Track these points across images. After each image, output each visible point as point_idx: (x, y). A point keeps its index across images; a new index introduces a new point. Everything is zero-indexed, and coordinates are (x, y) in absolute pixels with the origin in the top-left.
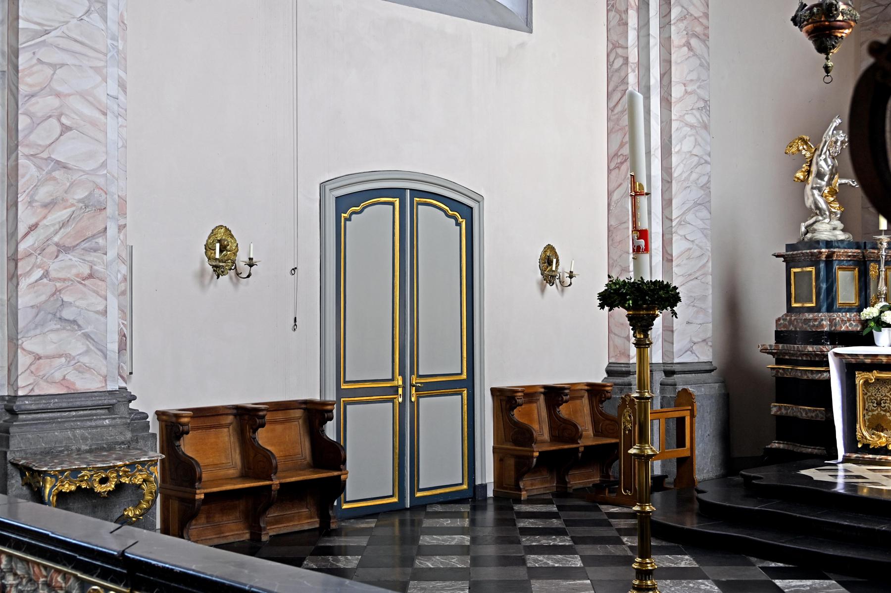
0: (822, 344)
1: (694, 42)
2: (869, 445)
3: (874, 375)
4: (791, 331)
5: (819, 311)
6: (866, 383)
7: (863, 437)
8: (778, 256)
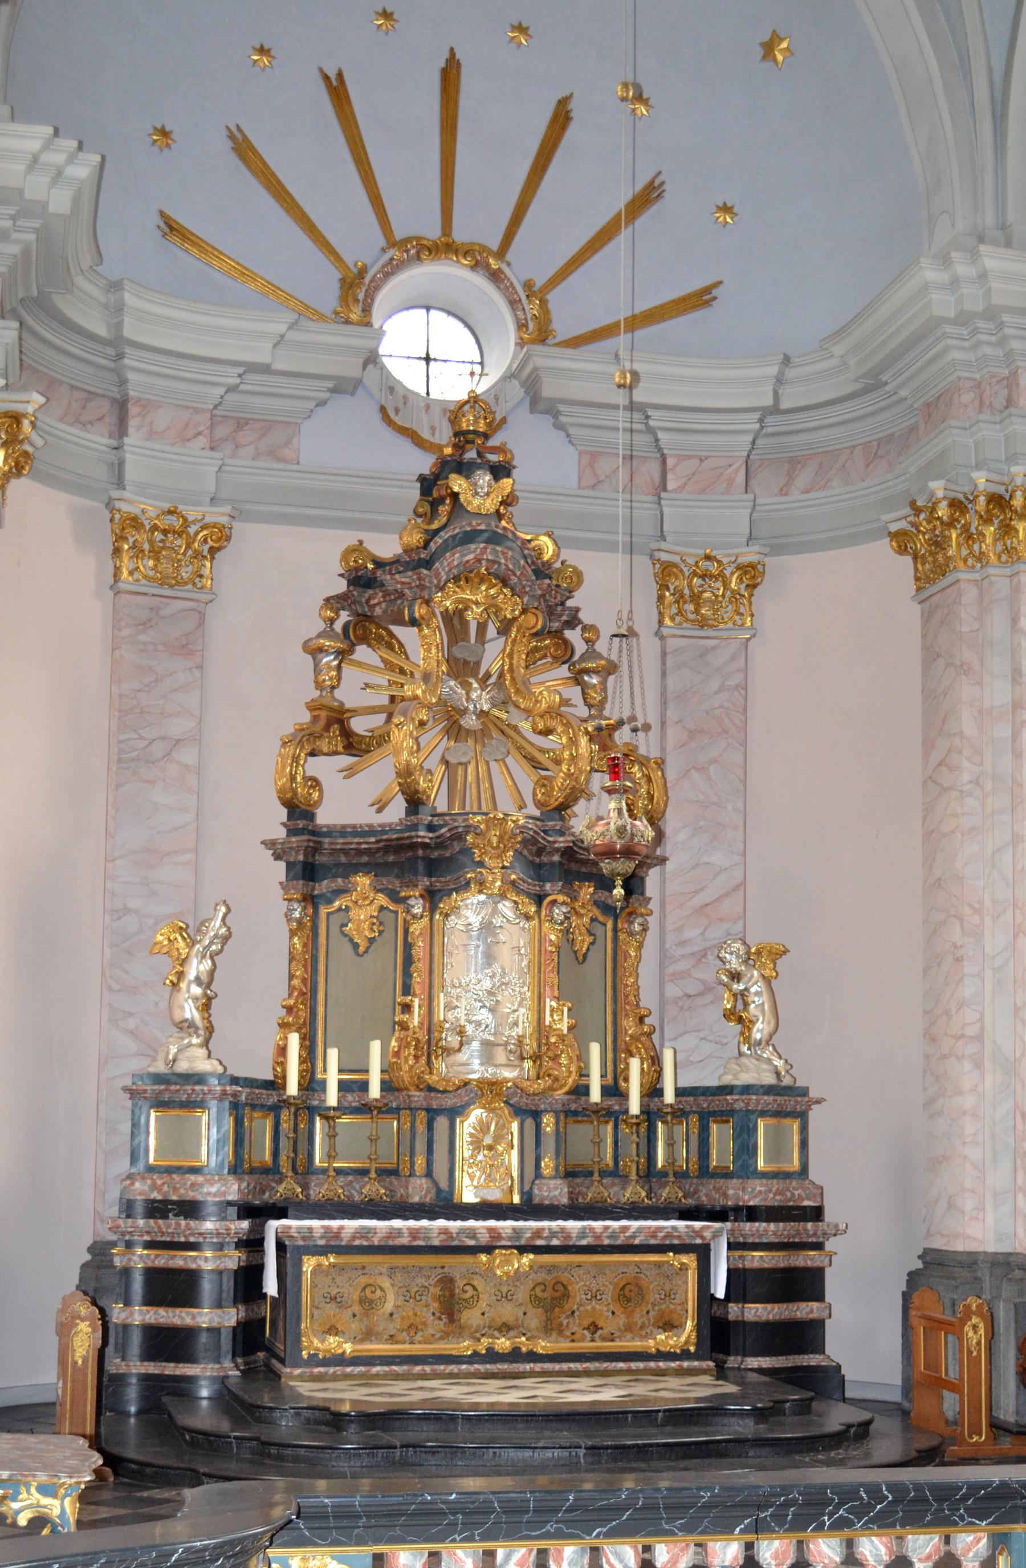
6: (317, 1269)
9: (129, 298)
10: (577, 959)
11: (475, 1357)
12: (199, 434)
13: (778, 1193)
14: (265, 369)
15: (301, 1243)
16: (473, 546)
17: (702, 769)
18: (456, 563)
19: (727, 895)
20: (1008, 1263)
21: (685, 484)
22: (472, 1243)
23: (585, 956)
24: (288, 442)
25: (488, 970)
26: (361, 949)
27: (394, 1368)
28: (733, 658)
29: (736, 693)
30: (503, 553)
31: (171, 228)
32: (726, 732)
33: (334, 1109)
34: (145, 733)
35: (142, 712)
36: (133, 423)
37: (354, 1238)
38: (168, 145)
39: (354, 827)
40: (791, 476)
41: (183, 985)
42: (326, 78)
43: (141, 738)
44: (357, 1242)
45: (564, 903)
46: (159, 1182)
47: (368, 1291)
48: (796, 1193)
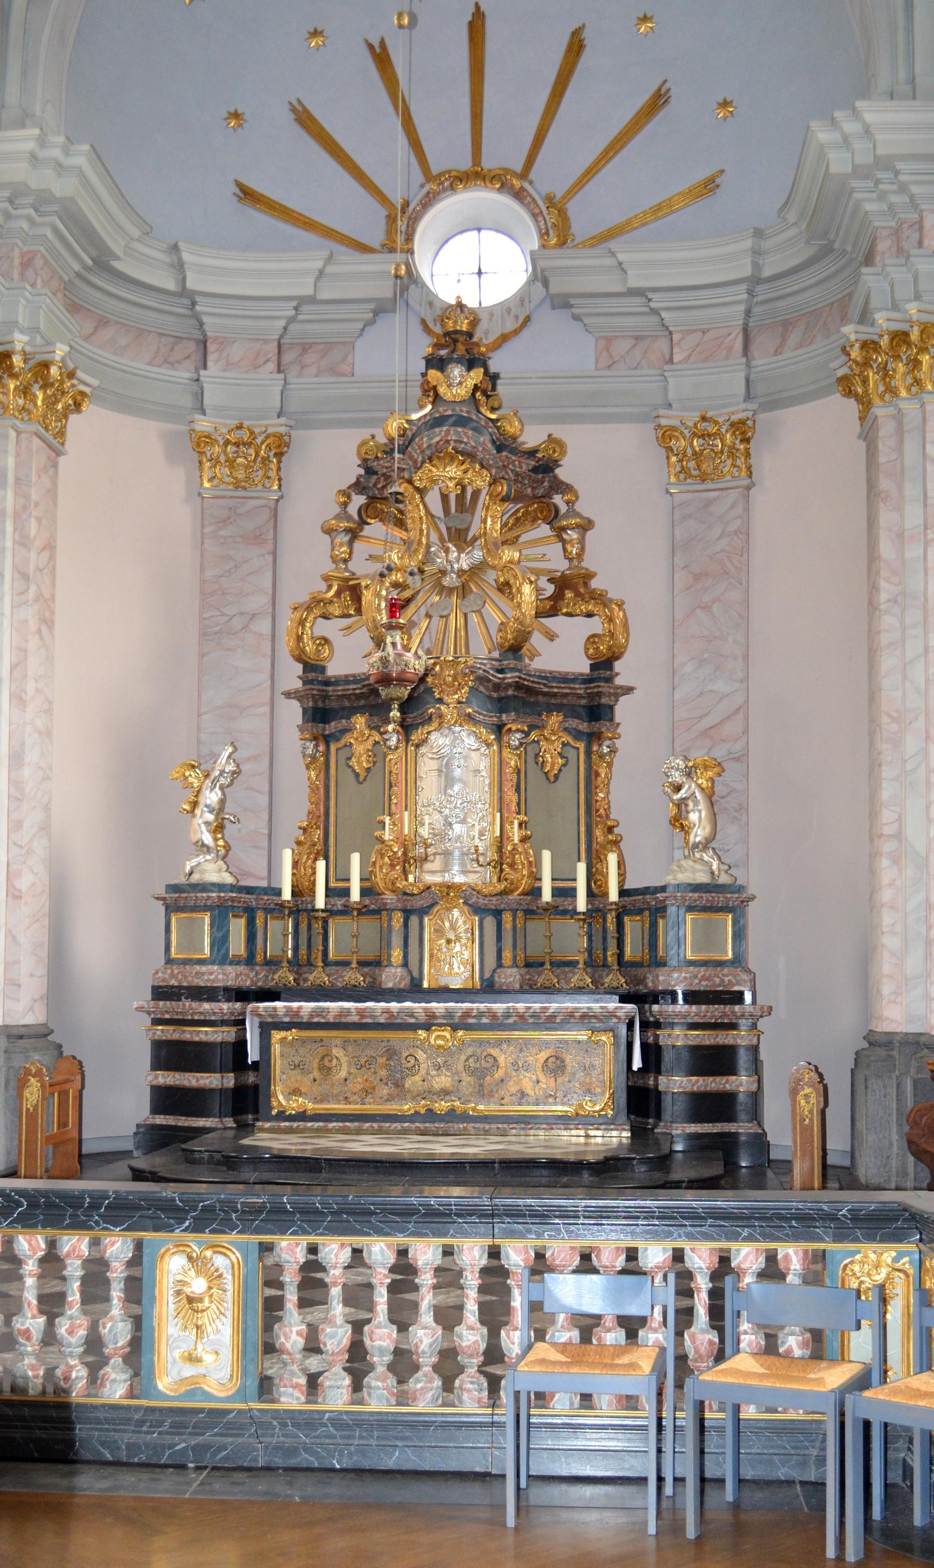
0: (219, 1001)
1: (44, 629)
2: (284, 1112)
3: (291, 1035)
4: (173, 987)
5: (213, 963)
7: (280, 1104)
8: (157, 898)
9: (186, 256)
10: (548, 778)
11: (415, 1117)
12: (268, 360)
13: (703, 978)
14: (311, 300)
15: (270, 1020)
16: (437, 430)
17: (706, 608)
18: (425, 446)
19: (729, 718)
20: (918, 1043)
21: (690, 355)
22: (412, 1021)
23: (556, 777)
24: (345, 358)
25: (455, 792)
26: (361, 778)
27: (348, 1124)
28: (733, 507)
29: (735, 538)
30: (465, 434)
31: (247, 195)
32: (727, 573)
33: (323, 911)
34: (227, 610)
35: (223, 594)
36: (211, 358)
37: (311, 1016)
38: (240, 126)
39: (354, 676)
40: (784, 338)
41: (198, 812)
42: (371, 47)
43: (223, 614)
44: (315, 1020)
45: (518, 730)
46: (176, 971)
47: (326, 1060)
48: (726, 979)
